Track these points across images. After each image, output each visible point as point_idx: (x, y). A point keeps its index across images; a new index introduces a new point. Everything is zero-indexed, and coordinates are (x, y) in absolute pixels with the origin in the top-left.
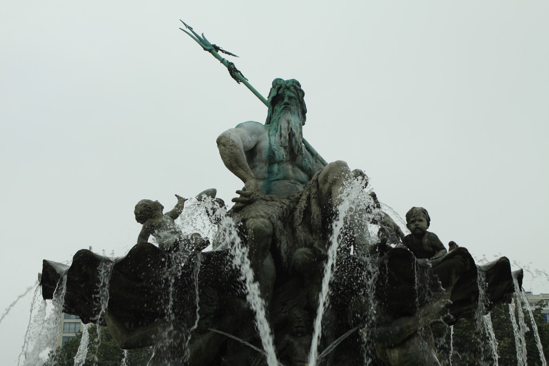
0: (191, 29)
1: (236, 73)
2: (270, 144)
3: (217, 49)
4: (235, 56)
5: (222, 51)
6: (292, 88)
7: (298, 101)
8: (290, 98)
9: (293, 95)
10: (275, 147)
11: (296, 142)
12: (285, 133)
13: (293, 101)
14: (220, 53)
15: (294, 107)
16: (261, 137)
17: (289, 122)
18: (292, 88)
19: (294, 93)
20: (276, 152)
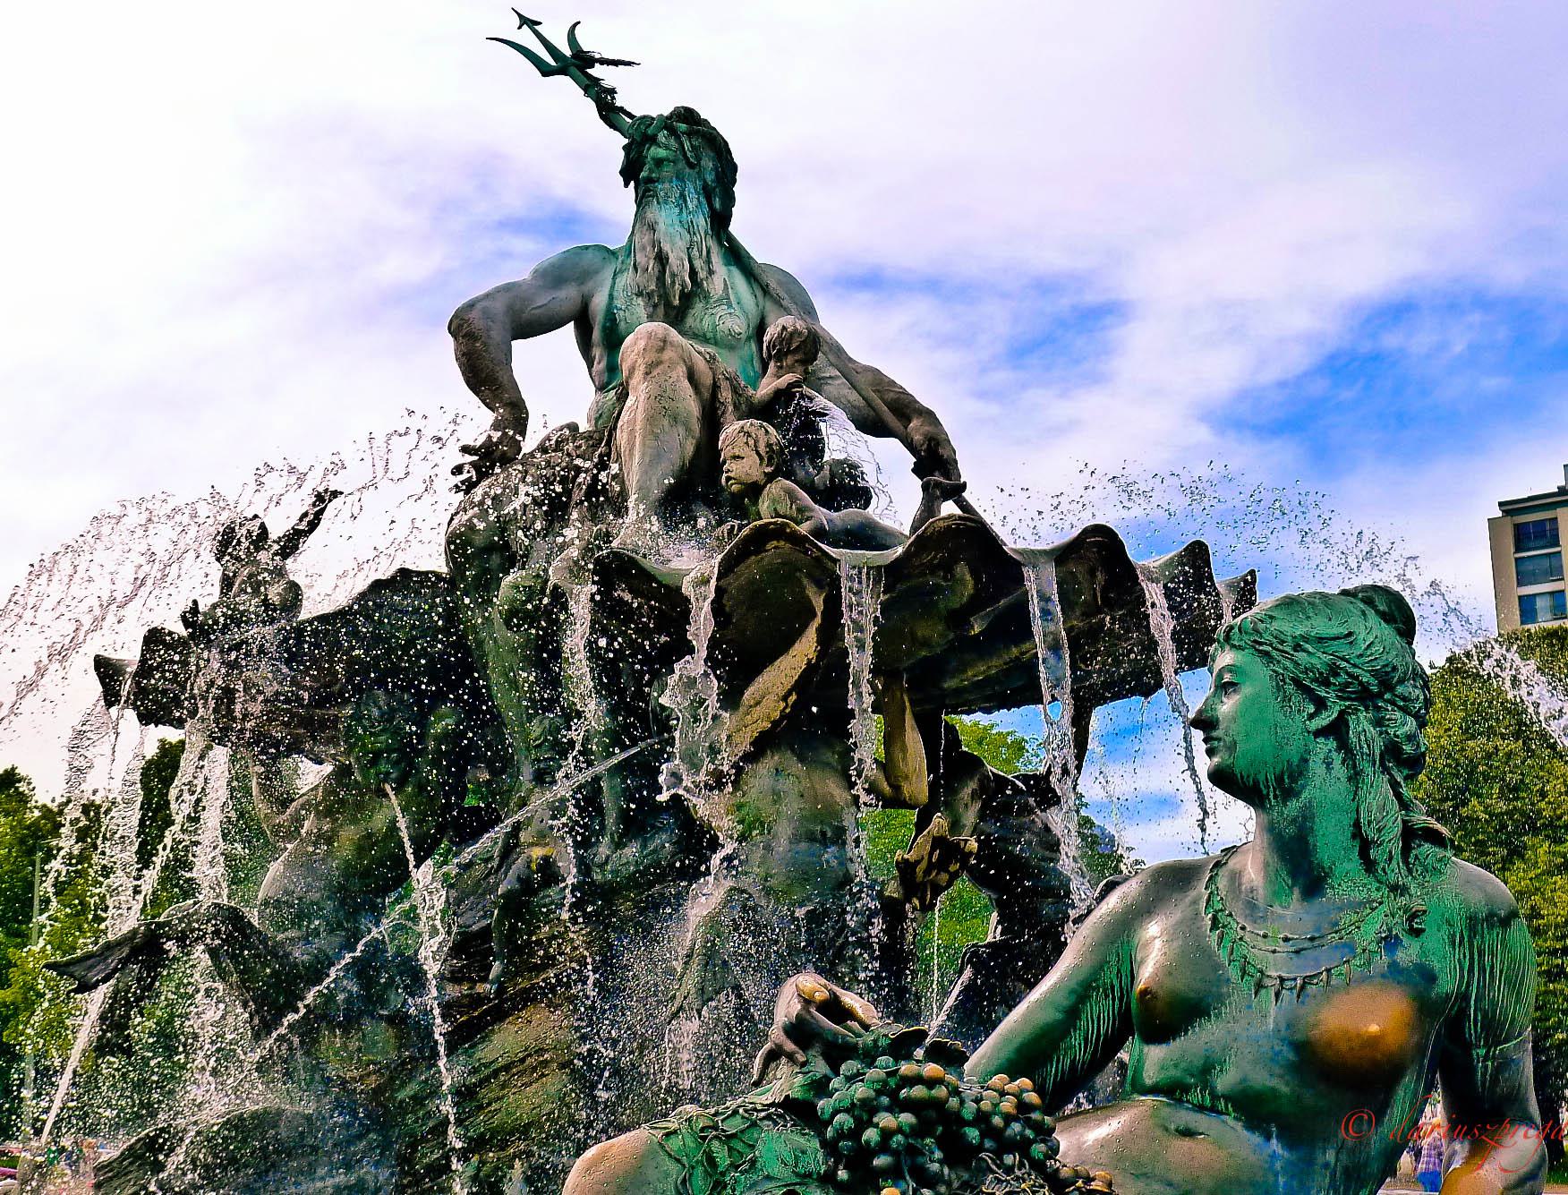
0: (532, 24)
1: (612, 115)
2: (611, 297)
4: (629, 64)
5: (604, 62)
6: (662, 136)
7: (682, 164)
8: (659, 162)
9: (662, 153)
10: (618, 303)
11: (673, 275)
12: (645, 259)
13: (668, 170)
15: (667, 185)
16: (590, 284)
17: (652, 228)
19: (667, 147)
20: (620, 315)
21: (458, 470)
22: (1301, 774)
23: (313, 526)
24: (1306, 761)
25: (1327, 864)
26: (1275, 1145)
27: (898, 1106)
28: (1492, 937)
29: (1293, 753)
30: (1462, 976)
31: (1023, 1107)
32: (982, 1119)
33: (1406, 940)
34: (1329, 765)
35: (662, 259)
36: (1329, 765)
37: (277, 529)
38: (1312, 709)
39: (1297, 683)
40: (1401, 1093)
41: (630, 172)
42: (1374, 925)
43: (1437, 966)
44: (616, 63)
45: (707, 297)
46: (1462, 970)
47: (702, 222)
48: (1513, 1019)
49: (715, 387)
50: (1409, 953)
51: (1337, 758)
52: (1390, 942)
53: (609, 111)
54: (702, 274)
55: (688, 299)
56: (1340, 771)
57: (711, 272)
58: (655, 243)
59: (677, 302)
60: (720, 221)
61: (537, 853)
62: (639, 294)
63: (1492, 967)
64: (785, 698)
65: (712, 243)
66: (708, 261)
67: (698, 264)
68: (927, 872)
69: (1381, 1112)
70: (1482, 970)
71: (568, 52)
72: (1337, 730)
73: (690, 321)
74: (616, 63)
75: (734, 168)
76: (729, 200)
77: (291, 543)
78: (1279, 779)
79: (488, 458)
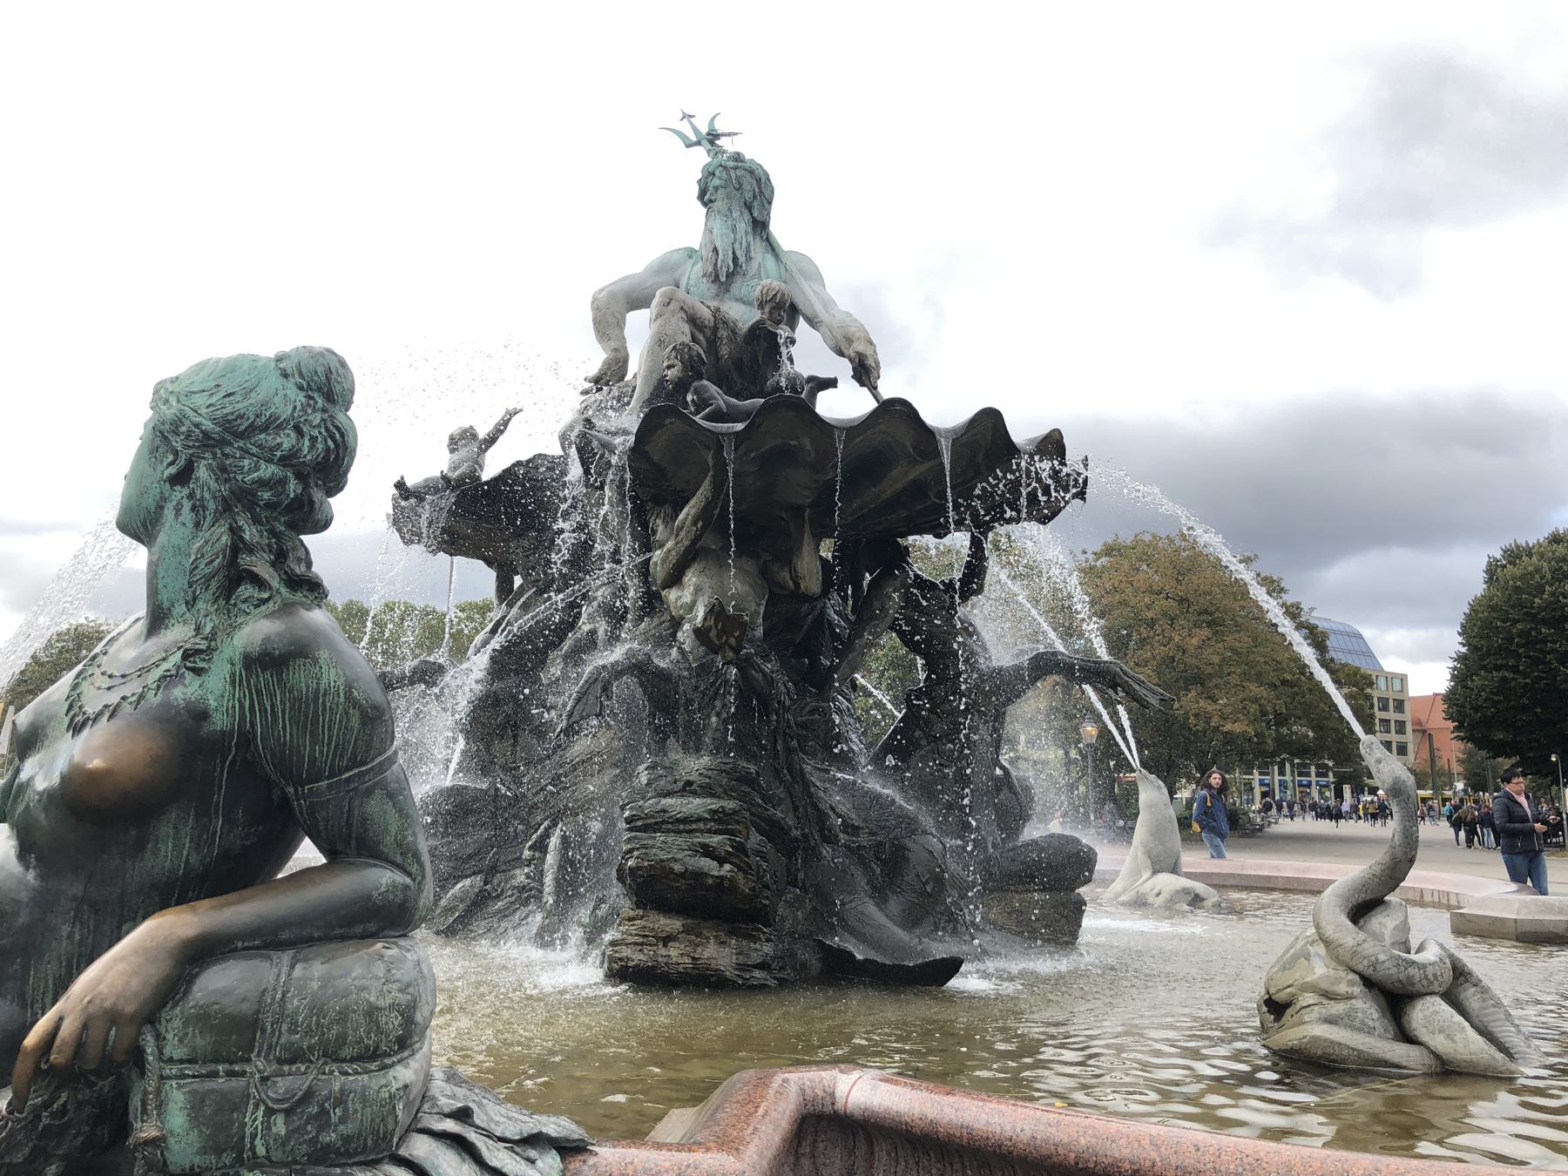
3: (713, 137)
8: (716, 189)
9: (716, 182)
13: (721, 192)
14: (721, 142)
22: (158, 520)
23: (502, 432)
24: (162, 508)
25: (166, 604)
26: (31, 876)
28: (265, 678)
29: (150, 502)
30: (242, 716)
33: (189, 676)
34: (178, 510)
35: (715, 250)
36: (178, 510)
37: (482, 435)
38: (171, 458)
40: (166, 830)
43: (213, 703)
44: (729, 135)
46: (242, 707)
47: (743, 226)
48: (313, 760)
49: (716, 329)
50: (187, 691)
51: (187, 505)
54: (742, 260)
55: (730, 276)
56: (187, 515)
57: (749, 259)
58: (712, 242)
60: (760, 226)
61: (586, 628)
63: (273, 706)
64: (695, 523)
66: (748, 250)
67: (738, 253)
68: (719, 637)
69: (140, 847)
70: (263, 710)
71: (704, 130)
72: (182, 477)
74: (729, 135)
78: (144, 525)
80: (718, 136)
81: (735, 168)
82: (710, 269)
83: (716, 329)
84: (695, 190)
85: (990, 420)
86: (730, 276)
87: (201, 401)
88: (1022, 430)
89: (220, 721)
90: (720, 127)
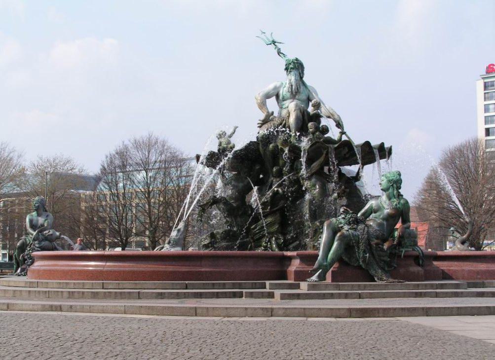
3: (274, 42)
9: (292, 67)
10: (284, 93)
14: (276, 44)
17: (290, 80)
18: (292, 64)
21: (258, 124)
23: (234, 133)
27: (353, 218)
31: (363, 219)
32: (359, 219)
35: (292, 86)
37: (228, 133)
39: (389, 181)
41: (286, 69)
42: (395, 203)
44: (280, 43)
45: (300, 92)
52: (396, 205)
53: (279, 53)
54: (299, 89)
59: (294, 94)
60: (301, 78)
62: (288, 92)
65: (300, 82)
72: (392, 185)
73: (297, 97)
74: (280, 43)
75: (304, 68)
76: (303, 73)
77: (230, 136)
79: (265, 122)
80: (275, 42)
81: (297, 63)
82: (290, 90)
83: (304, 112)
84: (284, 67)
85: (382, 145)
86: (296, 92)
87: (393, 178)
88: (386, 146)
89: (401, 209)
90: (276, 40)
